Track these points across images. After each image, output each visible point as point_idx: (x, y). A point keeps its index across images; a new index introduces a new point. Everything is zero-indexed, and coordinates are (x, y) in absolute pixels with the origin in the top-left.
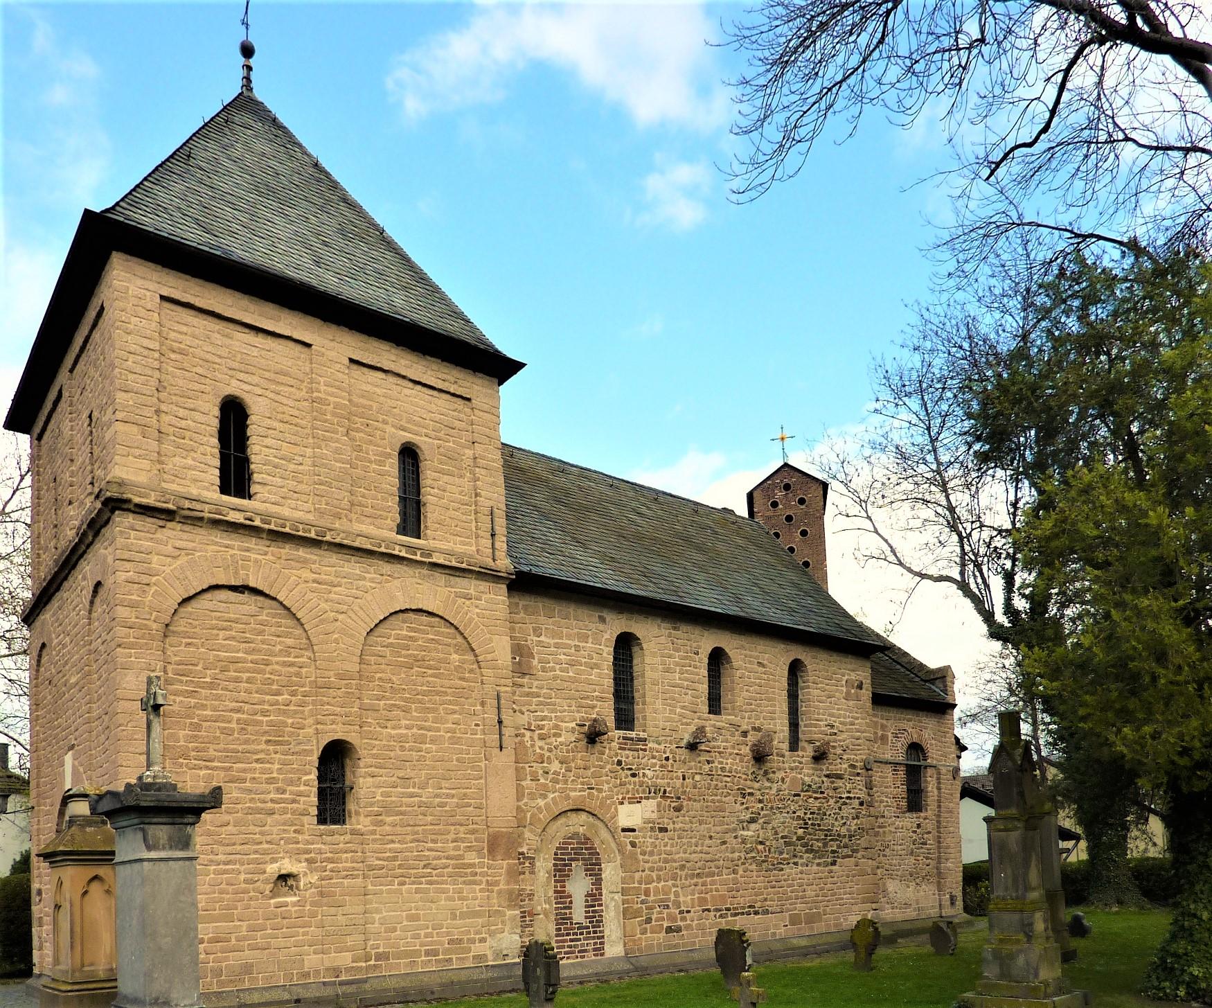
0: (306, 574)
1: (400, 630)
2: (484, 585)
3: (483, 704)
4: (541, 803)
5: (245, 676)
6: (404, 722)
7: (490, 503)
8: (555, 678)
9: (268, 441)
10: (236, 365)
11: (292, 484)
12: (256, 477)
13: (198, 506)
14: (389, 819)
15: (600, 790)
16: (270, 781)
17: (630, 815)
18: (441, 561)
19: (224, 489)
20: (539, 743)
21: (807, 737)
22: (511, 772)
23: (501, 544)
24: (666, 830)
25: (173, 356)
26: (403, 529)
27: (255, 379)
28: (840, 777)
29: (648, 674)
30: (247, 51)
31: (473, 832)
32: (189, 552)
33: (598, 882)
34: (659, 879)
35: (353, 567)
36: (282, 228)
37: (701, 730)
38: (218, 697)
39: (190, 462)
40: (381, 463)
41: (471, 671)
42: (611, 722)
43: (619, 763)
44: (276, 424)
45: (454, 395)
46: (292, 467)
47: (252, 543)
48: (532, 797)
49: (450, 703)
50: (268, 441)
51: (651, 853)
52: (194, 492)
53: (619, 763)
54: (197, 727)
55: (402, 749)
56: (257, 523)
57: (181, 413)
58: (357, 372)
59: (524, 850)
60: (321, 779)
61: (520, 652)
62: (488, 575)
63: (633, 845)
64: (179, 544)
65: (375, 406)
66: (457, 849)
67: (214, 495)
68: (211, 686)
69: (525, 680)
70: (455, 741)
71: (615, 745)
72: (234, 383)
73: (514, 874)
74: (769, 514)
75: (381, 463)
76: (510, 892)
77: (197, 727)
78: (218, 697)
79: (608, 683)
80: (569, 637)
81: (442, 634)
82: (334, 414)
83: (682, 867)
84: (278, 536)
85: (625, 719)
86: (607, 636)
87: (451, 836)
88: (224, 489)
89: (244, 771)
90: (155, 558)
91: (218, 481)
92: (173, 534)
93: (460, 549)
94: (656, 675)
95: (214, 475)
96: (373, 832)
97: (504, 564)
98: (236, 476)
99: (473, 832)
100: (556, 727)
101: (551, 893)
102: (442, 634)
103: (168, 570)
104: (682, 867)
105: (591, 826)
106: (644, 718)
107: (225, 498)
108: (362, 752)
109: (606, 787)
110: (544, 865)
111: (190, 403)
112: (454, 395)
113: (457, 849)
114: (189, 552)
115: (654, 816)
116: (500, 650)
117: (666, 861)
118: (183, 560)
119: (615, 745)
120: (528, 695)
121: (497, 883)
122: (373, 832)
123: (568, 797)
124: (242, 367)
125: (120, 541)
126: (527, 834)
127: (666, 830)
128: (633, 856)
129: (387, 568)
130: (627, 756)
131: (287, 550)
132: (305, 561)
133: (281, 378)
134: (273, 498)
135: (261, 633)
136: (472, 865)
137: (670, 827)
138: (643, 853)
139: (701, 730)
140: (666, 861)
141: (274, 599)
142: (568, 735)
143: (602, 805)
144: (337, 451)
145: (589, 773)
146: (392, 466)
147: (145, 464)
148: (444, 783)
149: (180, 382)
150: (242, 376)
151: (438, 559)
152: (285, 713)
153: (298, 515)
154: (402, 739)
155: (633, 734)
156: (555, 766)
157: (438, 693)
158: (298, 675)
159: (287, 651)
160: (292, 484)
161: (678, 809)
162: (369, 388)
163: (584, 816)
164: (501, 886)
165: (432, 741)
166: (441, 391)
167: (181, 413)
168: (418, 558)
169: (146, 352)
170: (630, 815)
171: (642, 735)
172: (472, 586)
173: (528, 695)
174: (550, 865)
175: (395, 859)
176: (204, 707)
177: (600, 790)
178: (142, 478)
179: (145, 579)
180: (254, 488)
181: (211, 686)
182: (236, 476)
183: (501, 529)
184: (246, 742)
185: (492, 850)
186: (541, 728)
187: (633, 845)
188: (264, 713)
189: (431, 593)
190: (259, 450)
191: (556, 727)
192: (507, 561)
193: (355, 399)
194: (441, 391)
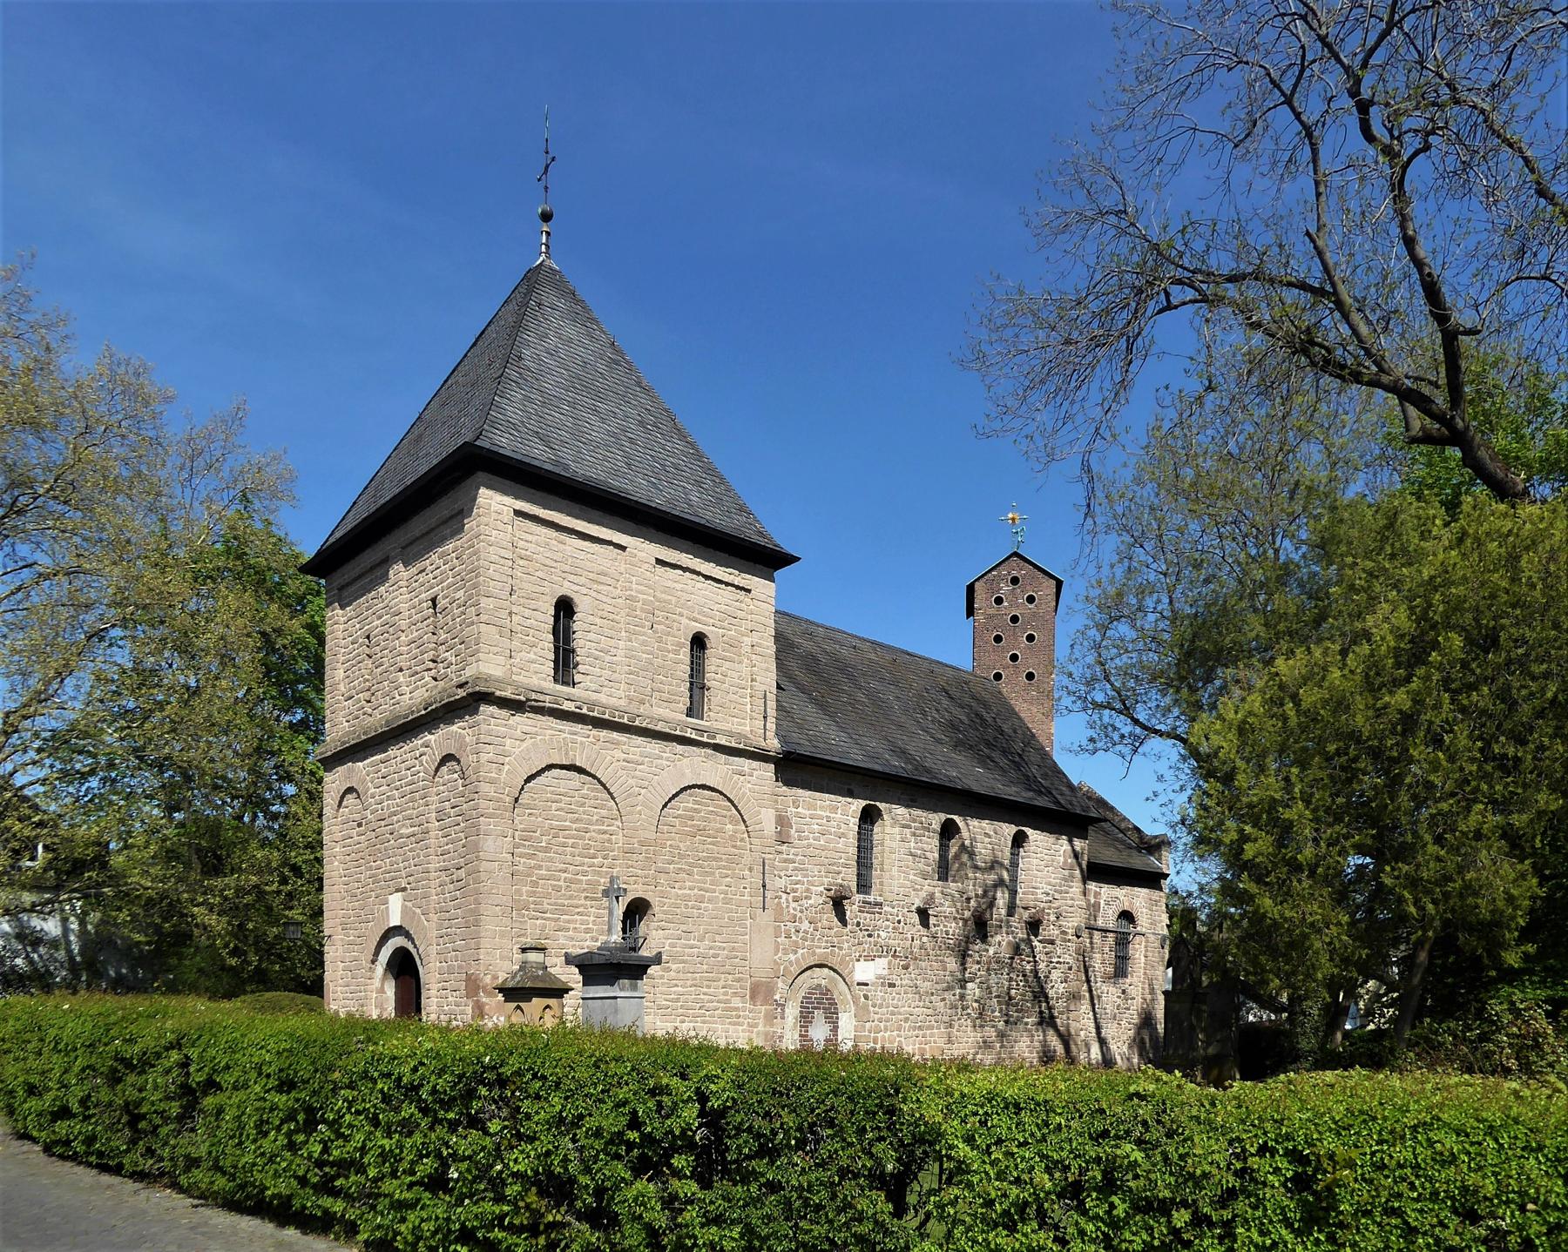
0: (618, 754)
1: (687, 802)
2: (755, 764)
3: (751, 870)
4: (792, 957)
5: (570, 841)
6: (688, 884)
7: (763, 688)
8: (809, 846)
9: (591, 636)
10: (567, 568)
11: (607, 673)
13: (541, 697)
14: (674, 967)
15: (841, 949)
16: (587, 931)
17: (865, 971)
18: (723, 742)
19: (556, 681)
20: (794, 905)
21: (1024, 903)
22: (771, 931)
23: (771, 726)
24: (892, 985)
25: (522, 562)
26: (690, 713)
27: (582, 580)
28: (1052, 942)
29: (887, 843)
31: (739, 980)
32: (533, 735)
33: (835, 1029)
34: (886, 1030)
35: (654, 747)
36: (598, 431)
37: (932, 896)
38: (551, 860)
39: (532, 656)
40: (677, 652)
41: (742, 840)
42: (854, 890)
43: (858, 924)
44: (598, 621)
45: (738, 587)
46: (608, 658)
47: (578, 727)
48: (786, 953)
49: (725, 868)
50: (591, 636)
51: (881, 1006)
53: (858, 924)
54: (535, 884)
55: (686, 906)
56: (584, 711)
57: (527, 613)
58: (660, 570)
59: (777, 997)
61: (782, 821)
62: (759, 756)
63: (866, 997)
64: (528, 729)
65: (674, 600)
66: (726, 994)
67: (549, 685)
68: (546, 850)
69: (784, 847)
70: (727, 901)
72: (566, 584)
73: (770, 1018)
74: (991, 611)
75: (677, 652)
76: (766, 1034)
77: (535, 884)
78: (551, 860)
79: (853, 851)
80: (822, 808)
81: (719, 807)
82: (642, 610)
83: (906, 1020)
84: (599, 723)
85: (864, 886)
86: (853, 807)
87: (722, 983)
89: (568, 922)
90: (508, 742)
91: (552, 672)
92: (522, 721)
93: (739, 729)
94: (894, 845)
95: (549, 667)
96: (662, 977)
97: (773, 744)
99: (739, 980)
100: (808, 890)
101: (797, 1036)
102: (719, 807)
103: (517, 751)
104: (906, 1020)
105: (832, 980)
106: (881, 884)
107: (559, 687)
108: (656, 909)
109: (846, 945)
110: (792, 1011)
111: (533, 605)
112: (738, 587)
113: (726, 994)
114: (533, 735)
115: (885, 972)
116: (766, 820)
117: (893, 1014)
118: (529, 742)
120: (785, 861)
121: (756, 1026)
122: (662, 977)
123: (814, 954)
124: (573, 570)
125: (484, 727)
126: (780, 984)
127: (892, 985)
128: (865, 1007)
129: (680, 748)
130: (866, 918)
131: (604, 734)
132: (618, 743)
133: (602, 579)
134: (594, 686)
135: (583, 805)
136: (737, 1009)
137: (898, 983)
139: (932, 896)
140: (893, 1014)
141: (594, 777)
142: (818, 899)
143: (842, 962)
144: (644, 643)
145: (832, 932)
146: (685, 655)
147: (501, 660)
148: (717, 938)
149: (525, 585)
150: (572, 578)
151: (721, 740)
152: (599, 873)
153: (613, 701)
154: (686, 898)
155: (871, 898)
156: (805, 925)
157: (715, 859)
158: (609, 841)
159: (601, 821)
160: (607, 673)
161: (906, 967)
162: (669, 584)
163: (826, 970)
164: (761, 1028)
165: (710, 901)
166: (727, 584)
167: (527, 613)
168: (705, 739)
169: (503, 561)
170: (865, 971)
171: (880, 899)
172: (746, 764)
173: (785, 861)
174: (797, 1012)
175: (677, 1000)
176: (540, 867)
177: (841, 949)
178: (497, 672)
179: (501, 759)
180: (577, 678)
181: (546, 850)
183: (772, 712)
184: (571, 897)
185: (753, 997)
186: (795, 891)
187: (866, 997)
188: (585, 873)
189: (715, 769)
190: (583, 642)
191: (808, 890)
192: (776, 741)
193: (658, 594)
194: (727, 584)
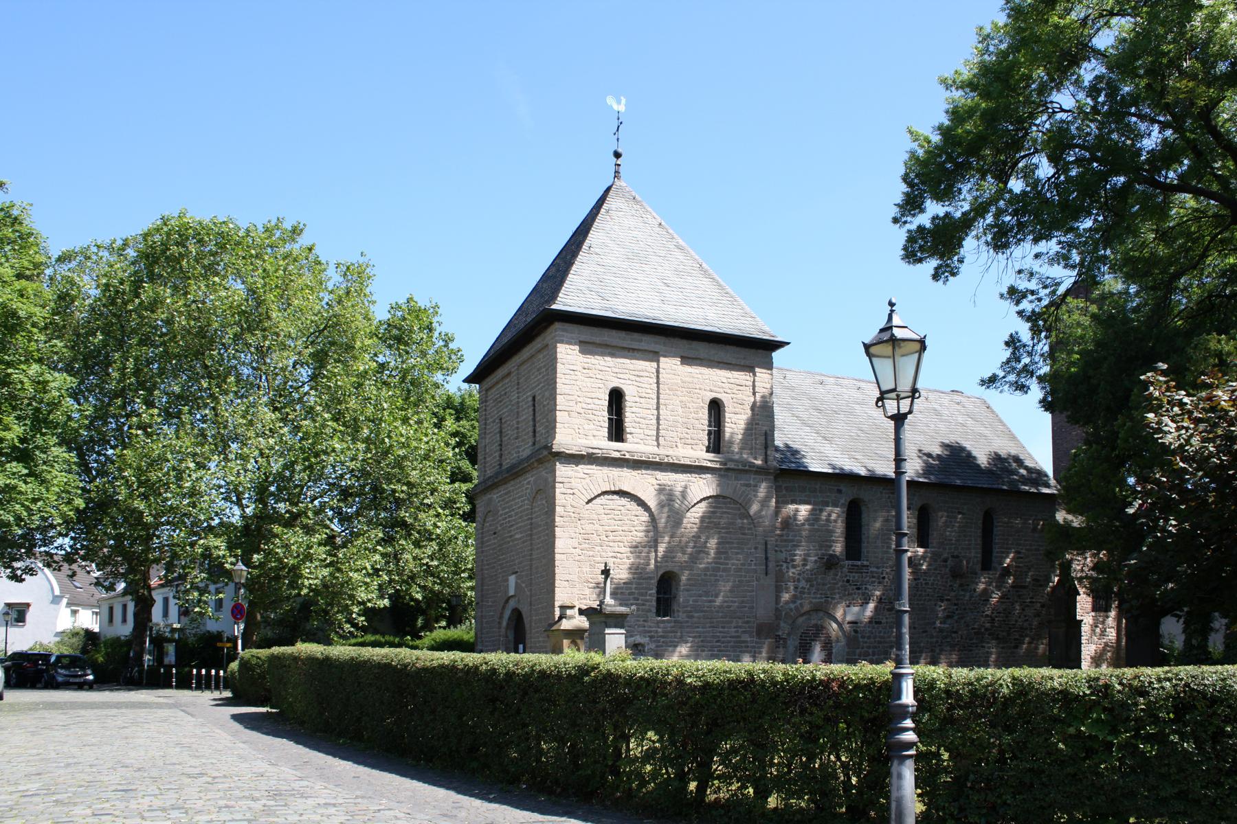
4: (792, 606)
9: (634, 409)
12: (628, 430)
30: (617, 155)
52: (595, 443)
53: (848, 581)
60: (658, 592)
71: (845, 570)
88: (610, 438)
98: (617, 431)
119: (845, 570)
138: (863, 637)
140: (880, 642)
165: (724, 570)
167: (590, 401)
182: (617, 431)
